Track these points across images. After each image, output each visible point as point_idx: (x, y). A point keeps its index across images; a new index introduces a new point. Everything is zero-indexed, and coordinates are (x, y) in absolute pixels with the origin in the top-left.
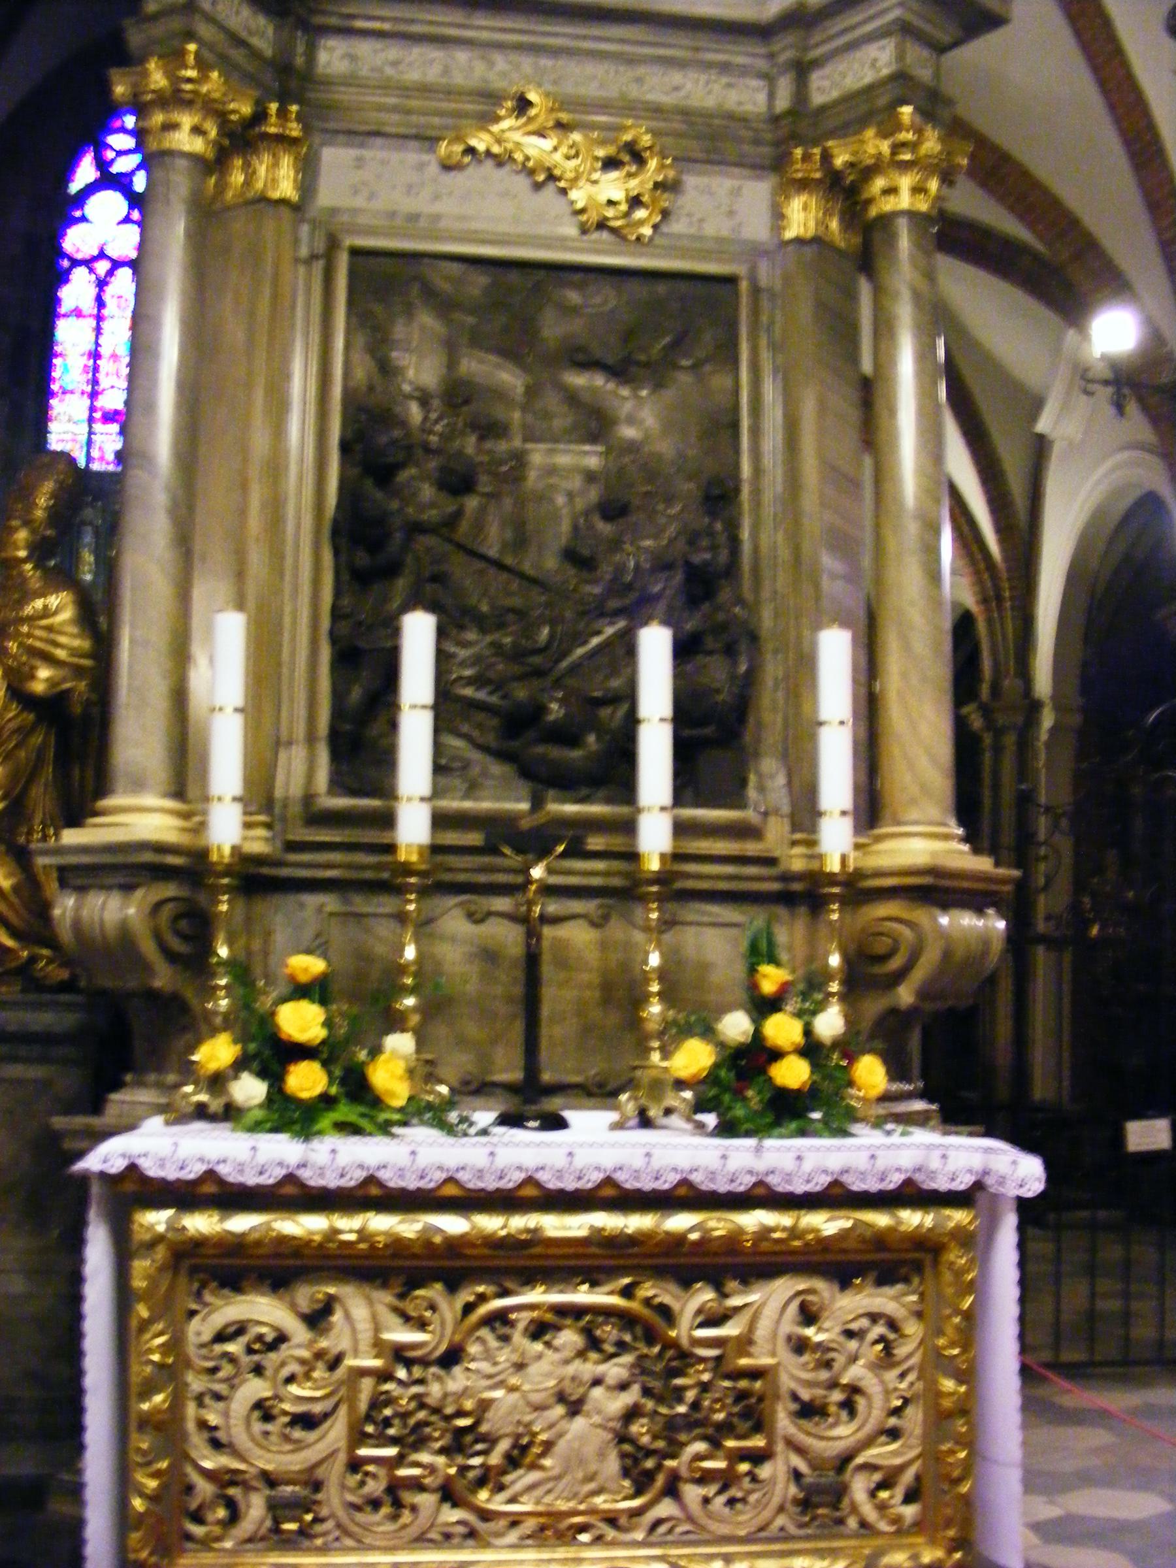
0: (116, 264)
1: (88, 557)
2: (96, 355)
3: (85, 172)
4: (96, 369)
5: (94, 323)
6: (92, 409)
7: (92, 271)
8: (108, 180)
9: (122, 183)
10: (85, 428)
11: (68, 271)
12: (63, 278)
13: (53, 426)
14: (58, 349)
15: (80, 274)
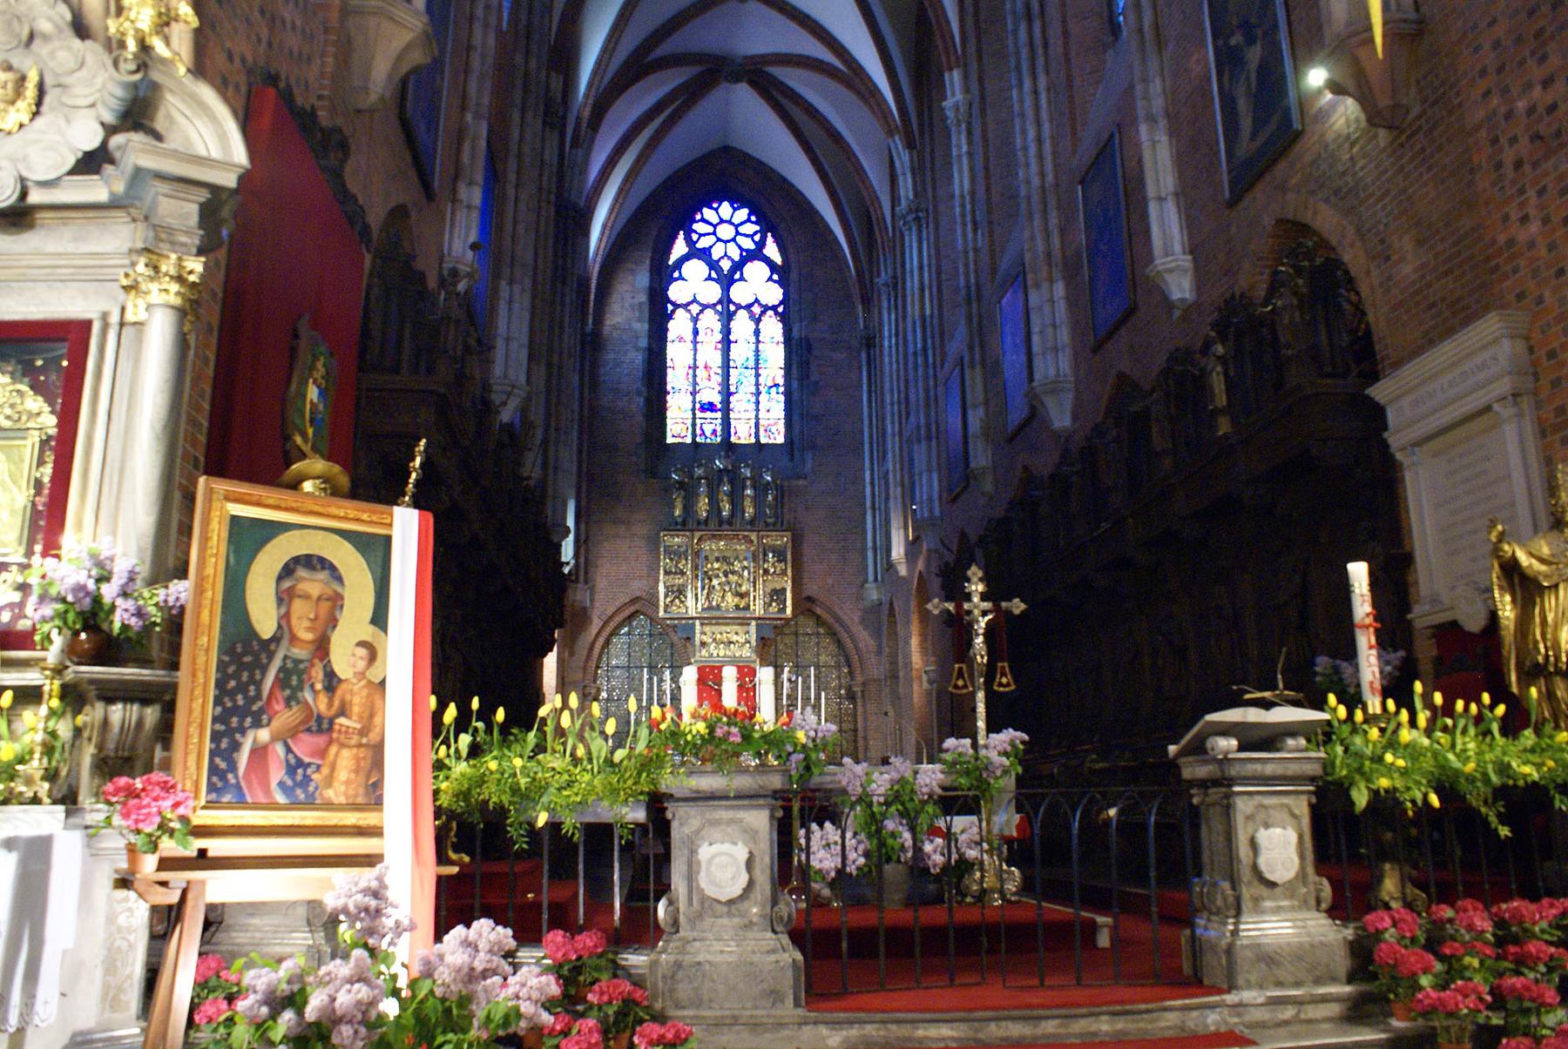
0: (705, 307)
2: (695, 367)
3: (680, 248)
4: (695, 376)
5: (691, 346)
6: (694, 402)
8: (695, 253)
9: (705, 254)
11: (673, 312)
12: (670, 317)
13: (669, 414)
15: (680, 312)
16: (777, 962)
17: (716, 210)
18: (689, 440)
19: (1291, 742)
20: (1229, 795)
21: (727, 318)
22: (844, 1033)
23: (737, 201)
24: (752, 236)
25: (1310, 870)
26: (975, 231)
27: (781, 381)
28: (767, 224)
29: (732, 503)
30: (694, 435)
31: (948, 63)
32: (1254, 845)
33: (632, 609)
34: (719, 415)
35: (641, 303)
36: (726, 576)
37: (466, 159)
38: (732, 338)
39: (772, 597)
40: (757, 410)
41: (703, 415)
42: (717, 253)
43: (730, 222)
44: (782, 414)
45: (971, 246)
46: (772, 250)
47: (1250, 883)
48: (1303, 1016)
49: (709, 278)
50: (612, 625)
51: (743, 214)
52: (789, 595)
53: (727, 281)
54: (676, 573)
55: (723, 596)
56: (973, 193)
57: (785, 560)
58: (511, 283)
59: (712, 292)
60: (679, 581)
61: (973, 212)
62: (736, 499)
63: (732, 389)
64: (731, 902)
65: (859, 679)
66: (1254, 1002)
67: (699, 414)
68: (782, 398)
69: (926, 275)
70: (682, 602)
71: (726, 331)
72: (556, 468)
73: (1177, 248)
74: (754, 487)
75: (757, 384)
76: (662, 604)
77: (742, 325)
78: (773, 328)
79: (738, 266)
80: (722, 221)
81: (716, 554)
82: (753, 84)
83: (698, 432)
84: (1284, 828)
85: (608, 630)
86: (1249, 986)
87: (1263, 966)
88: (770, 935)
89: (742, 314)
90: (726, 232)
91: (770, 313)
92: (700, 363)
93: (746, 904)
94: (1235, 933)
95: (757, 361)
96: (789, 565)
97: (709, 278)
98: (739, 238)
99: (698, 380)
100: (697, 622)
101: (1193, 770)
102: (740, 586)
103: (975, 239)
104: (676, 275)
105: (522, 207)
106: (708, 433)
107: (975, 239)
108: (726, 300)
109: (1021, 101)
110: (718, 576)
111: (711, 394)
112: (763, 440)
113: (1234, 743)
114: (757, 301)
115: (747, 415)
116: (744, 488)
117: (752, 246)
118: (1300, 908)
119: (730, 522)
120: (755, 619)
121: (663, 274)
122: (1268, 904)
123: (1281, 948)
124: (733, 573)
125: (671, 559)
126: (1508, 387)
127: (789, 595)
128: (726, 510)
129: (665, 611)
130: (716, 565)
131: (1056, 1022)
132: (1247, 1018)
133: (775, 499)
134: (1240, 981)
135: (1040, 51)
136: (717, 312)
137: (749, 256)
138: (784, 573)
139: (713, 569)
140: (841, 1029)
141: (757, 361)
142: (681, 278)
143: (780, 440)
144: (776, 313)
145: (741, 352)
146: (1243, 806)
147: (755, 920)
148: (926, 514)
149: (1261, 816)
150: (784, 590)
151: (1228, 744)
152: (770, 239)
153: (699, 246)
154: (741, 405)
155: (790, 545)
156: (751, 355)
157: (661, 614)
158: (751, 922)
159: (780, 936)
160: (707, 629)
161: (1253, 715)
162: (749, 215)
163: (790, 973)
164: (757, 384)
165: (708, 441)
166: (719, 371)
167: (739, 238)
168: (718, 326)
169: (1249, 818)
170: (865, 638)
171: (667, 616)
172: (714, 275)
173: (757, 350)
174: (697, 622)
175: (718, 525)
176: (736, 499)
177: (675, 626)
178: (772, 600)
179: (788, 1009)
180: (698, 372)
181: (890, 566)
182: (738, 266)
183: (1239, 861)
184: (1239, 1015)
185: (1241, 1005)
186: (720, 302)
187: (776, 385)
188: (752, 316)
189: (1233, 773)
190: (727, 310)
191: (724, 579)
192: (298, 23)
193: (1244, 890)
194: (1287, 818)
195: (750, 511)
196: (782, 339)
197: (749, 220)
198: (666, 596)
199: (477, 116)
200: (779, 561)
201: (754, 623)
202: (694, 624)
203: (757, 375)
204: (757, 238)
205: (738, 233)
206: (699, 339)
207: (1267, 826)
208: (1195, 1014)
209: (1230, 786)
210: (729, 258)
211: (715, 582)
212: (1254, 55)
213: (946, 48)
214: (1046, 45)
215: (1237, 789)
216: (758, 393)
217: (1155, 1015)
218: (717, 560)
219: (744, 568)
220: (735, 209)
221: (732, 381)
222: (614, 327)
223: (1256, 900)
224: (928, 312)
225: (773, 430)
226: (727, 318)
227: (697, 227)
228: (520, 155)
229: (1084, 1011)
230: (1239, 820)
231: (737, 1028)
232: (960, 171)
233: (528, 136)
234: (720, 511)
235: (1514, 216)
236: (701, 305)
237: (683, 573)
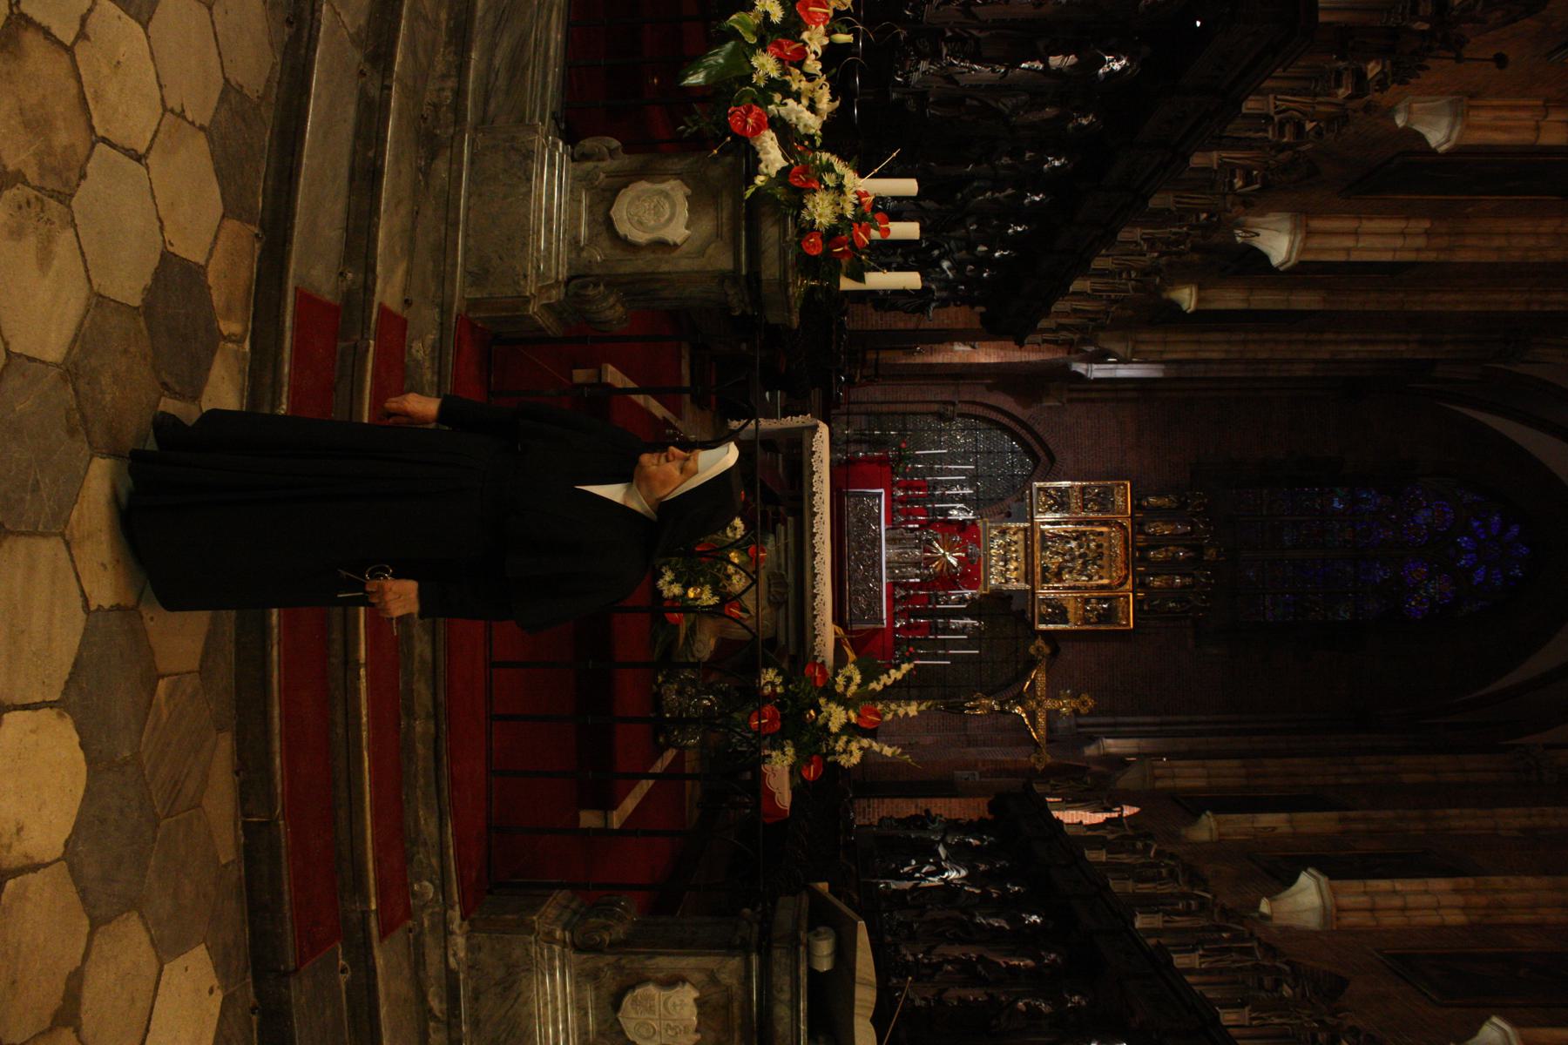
16: (525, 276)
20: (744, 949)
22: (427, 364)
29: (1165, 562)
32: (671, 982)
33: (1041, 454)
36: (1081, 556)
42: (1463, 541)
47: (619, 969)
48: (432, 1024)
50: (1023, 432)
52: (1061, 627)
55: (1058, 553)
57: (1099, 622)
62: (1170, 566)
64: (609, 223)
66: (450, 952)
70: (1050, 507)
72: (1198, 342)
74: (1183, 586)
76: (1048, 484)
84: (697, 1031)
85: (1017, 428)
86: (472, 948)
87: (499, 974)
88: (563, 273)
94: (551, 940)
100: (1027, 525)
101: (788, 911)
102: (1070, 572)
110: (1080, 546)
113: (824, 965)
116: (1182, 575)
119: (1143, 560)
120: (1033, 588)
122: (589, 995)
123: (525, 1003)
124: (1085, 564)
125: (1098, 494)
127: (1061, 627)
129: (1040, 489)
130: (1092, 545)
132: (429, 940)
133: (1170, 610)
134: (481, 937)
138: (1086, 621)
139: (1089, 541)
140: (433, 359)
147: (584, 254)
148: (1157, 772)
150: (1066, 622)
157: (1037, 484)
158: (582, 249)
159: (563, 289)
160: (1021, 536)
161: (865, 997)
171: (1034, 491)
174: (1027, 525)
176: (1170, 566)
177: (1023, 500)
179: (461, 291)
181: (1092, 739)
183: (651, 956)
184: (433, 927)
185: (448, 932)
189: (777, 953)
191: (1077, 553)
193: (610, 959)
198: (1058, 489)
200: (1099, 616)
201: (1028, 587)
202: (1026, 521)
208: (434, 861)
209: (759, 953)
211: (1073, 544)
215: (755, 959)
217: (435, 802)
218: (1099, 546)
223: (594, 976)
229: (442, 697)
230: (709, 962)
231: (443, 227)
234: (1155, 547)
237: (1084, 507)
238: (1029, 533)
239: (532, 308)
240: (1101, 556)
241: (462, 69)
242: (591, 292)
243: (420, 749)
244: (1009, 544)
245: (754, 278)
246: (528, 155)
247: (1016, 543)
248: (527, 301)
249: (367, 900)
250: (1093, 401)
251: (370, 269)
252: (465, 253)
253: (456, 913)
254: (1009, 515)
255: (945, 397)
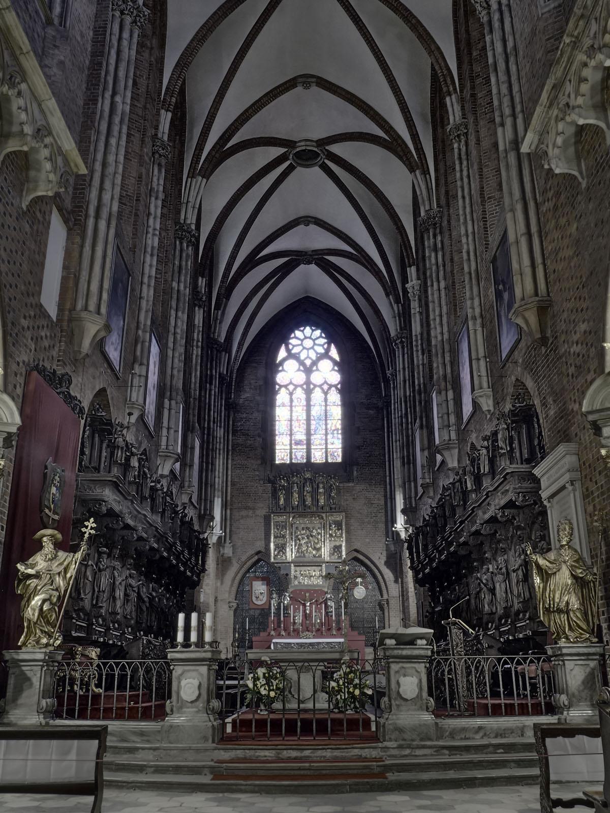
0: (296, 386)
1: (296, 495)
2: (291, 420)
3: (282, 353)
5: (289, 408)
6: (291, 440)
7: (287, 389)
8: (291, 355)
9: (296, 357)
10: (288, 447)
11: (279, 389)
14: (277, 418)
15: (283, 390)
17: (303, 331)
18: (288, 462)
19: (419, 642)
21: (308, 392)
23: (315, 325)
24: (322, 346)
25: (425, 694)
26: (423, 354)
27: (339, 427)
28: (332, 338)
30: (291, 459)
31: (409, 263)
32: (398, 683)
33: (256, 558)
34: (305, 447)
35: (260, 386)
36: (308, 538)
37: (138, 353)
38: (312, 403)
39: (334, 550)
40: (326, 444)
41: (295, 447)
42: (303, 356)
43: (310, 338)
44: (340, 446)
45: (421, 362)
46: (334, 353)
47: (395, 699)
48: (413, 754)
49: (299, 370)
51: (318, 333)
52: (343, 548)
53: (308, 371)
54: (280, 537)
56: (422, 334)
58: (170, 400)
59: (300, 378)
60: (281, 541)
61: (422, 344)
63: (312, 432)
64: (192, 702)
65: (385, 597)
67: (294, 447)
68: (340, 436)
69: (407, 373)
70: (284, 553)
71: (308, 400)
73: (485, 385)
74: (324, 487)
75: (326, 429)
77: (317, 395)
78: (335, 397)
79: (314, 363)
80: (306, 338)
81: (303, 526)
82: (317, 264)
83: (293, 457)
86: (390, 740)
87: (397, 733)
89: (318, 390)
90: (308, 343)
91: (333, 389)
92: (294, 418)
93: (197, 703)
95: (326, 416)
96: (344, 531)
97: (299, 370)
98: (316, 347)
99: (293, 427)
100: (292, 565)
103: (423, 359)
104: (280, 368)
105: (176, 360)
106: (299, 455)
107: (423, 359)
108: (308, 382)
109: (433, 294)
111: (301, 436)
112: (330, 461)
114: (326, 382)
115: (321, 447)
116: (318, 487)
117: (323, 351)
118: (418, 710)
121: (273, 367)
125: (278, 529)
126: (568, 477)
127: (343, 548)
128: (309, 501)
131: (310, 751)
132: (388, 753)
135: (441, 268)
136: (303, 389)
137: (321, 357)
141: (326, 416)
142: (283, 370)
143: (339, 460)
144: (337, 388)
145: (316, 411)
146: (394, 667)
149: (403, 671)
150: (341, 546)
151: (390, 642)
152: (333, 345)
153: (293, 352)
154: (317, 439)
155: (344, 520)
156: (323, 412)
157: (272, 560)
160: (298, 569)
162: (321, 334)
163: (211, 730)
164: (326, 429)
165: (299, 462)
166: (305, 422)
167: (316, 347)
168: (303, 396)
169: (397, 672)
170: (388, 574)
172: (302, 368)
173: (326, 411)
174: (292, 565)
175: (303, 511)
176: (315, 493)
178: (335, 551)
180: (293, 423)
182: (314, 363)
184: (385, 752)
185: (386, 748)
186: (305, 383)
187: (337, 430)
188: (322, 389)
190: (308, 389)
192: (48, 334)
193: (393, 702)
194: (414, 671)
195: (322, 502)
196: (340, 403)
197: (321, 336)
198: (275, 550)
199: (144, 331)
200: (338, 529)
201: (324, 565)
203: (326, 424)
204: (326, 346)
205: (315, 344)
206: (294, 404)
207: (405, 676)
210: (310, 358)
212: (506, 296)
213: (408, 255)
214: (444, 266)
215: (391, 660)
216: (326, 434)
218: (303, 529)
219: (318, 534)
220: (313, 331)
221: (313, 427)
222: (246, 399)
223: (398, 706)
224: (408, 394)
225: (336, 454)
226: (308, 392)
227: (293, 341)
228: (175, 333)
232: (415, 321)
233: (179, 323)
234: (304, 501)
235: (573, 399)
236: (294, 385)
238: (298, 564)
239: (215, 723)
240: (308, 528)
241: (143, 749)
242: (211, 707)
243: (335, 754)
244: (302, 575)
245: (210, 660)
246: (171, 726)
247: (301, 571)
248: (213, 725)
249: (373, 765)
250: (231, 531)
251: (204, 767)
252: (198, 743)
253: (380, 745)
254: (287, 575)
255: (226, 607)
